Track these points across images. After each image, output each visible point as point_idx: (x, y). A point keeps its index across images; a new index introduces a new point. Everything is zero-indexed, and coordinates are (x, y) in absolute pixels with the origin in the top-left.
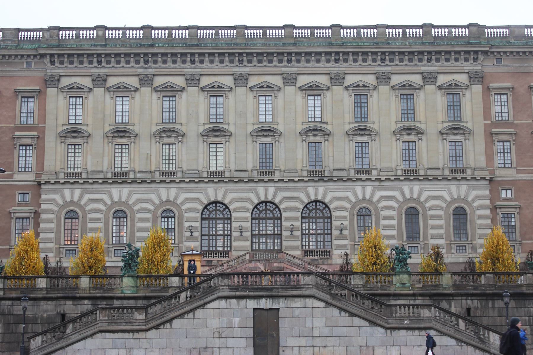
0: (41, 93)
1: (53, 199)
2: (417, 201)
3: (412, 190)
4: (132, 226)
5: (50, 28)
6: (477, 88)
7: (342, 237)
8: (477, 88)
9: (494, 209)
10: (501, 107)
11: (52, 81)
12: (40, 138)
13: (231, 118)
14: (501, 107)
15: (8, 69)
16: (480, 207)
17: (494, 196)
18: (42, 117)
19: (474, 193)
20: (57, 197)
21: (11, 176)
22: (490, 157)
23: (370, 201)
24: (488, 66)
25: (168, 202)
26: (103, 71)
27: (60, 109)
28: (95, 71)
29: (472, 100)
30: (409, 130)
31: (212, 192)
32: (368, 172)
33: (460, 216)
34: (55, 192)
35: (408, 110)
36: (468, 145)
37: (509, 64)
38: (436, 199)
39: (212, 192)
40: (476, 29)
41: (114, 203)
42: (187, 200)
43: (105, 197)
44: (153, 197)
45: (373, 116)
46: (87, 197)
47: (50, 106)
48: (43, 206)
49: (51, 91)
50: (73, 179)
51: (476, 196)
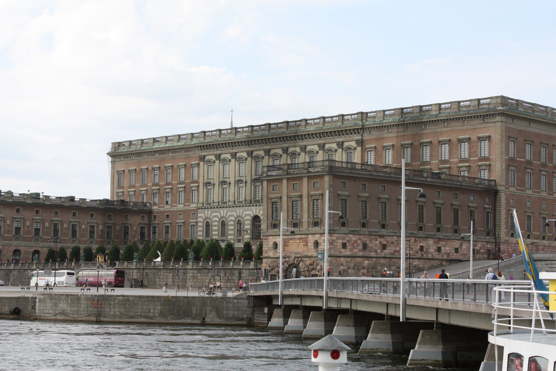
0: (198, 164)
1: (202, 215)
4: (228, 228)
6: (359, 149)
12: (198, 186)
15: (188, 153)
20: (203, 215)
21: (189, 205)
27: (201, 173)
28: (216, 152)
34: (202, 213)
37: (375, 134)
40: (363, 115)
41: (221, 217)
43: (218, 214)
44: (234, 213)
46: (213, 214)
47: (201, 171)
48: (199, 220)
49: (202, 163)
50: (208, 205)
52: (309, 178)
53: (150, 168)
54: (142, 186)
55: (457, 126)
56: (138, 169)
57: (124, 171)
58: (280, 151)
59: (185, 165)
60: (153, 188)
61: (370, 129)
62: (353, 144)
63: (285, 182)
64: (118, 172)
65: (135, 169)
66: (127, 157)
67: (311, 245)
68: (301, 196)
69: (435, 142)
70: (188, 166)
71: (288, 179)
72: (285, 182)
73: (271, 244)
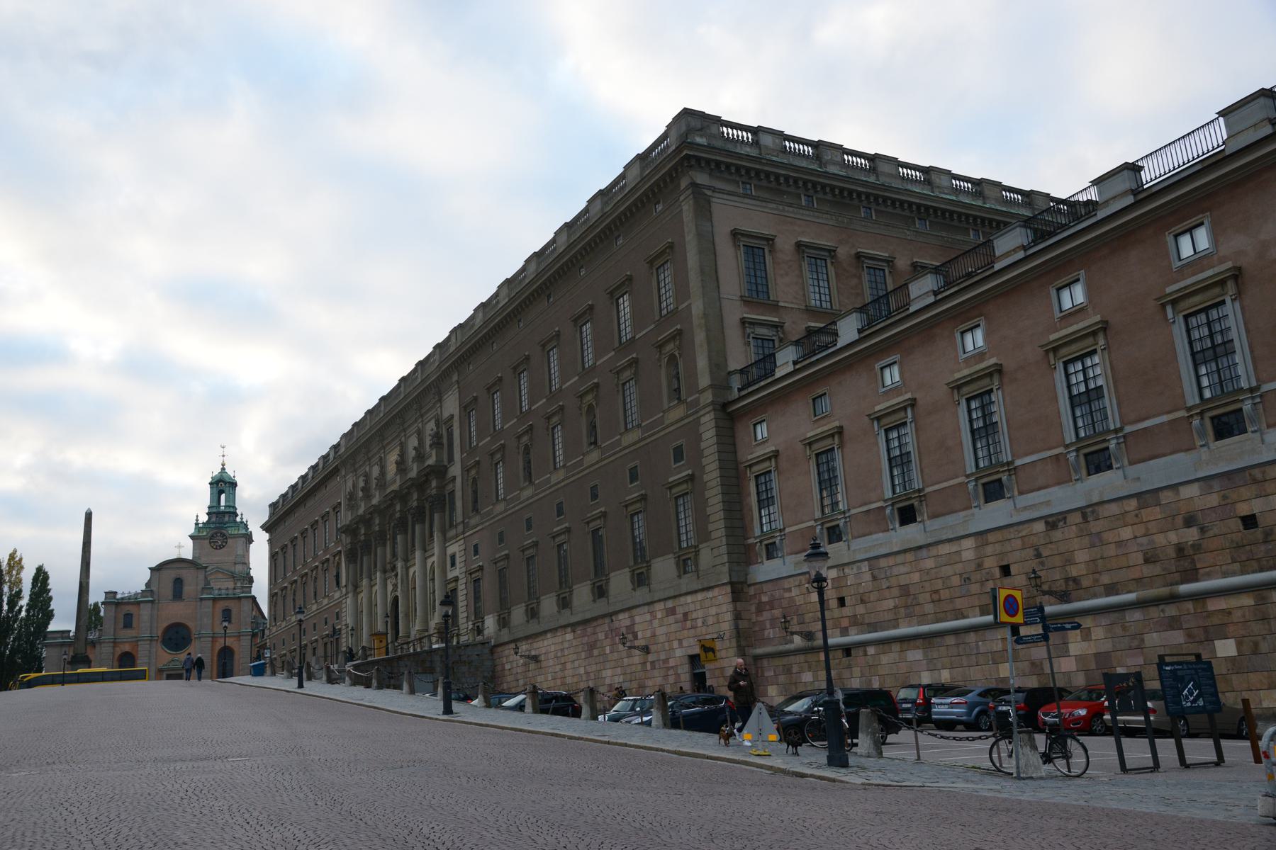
57: (770, 240)
64: (735, 234)
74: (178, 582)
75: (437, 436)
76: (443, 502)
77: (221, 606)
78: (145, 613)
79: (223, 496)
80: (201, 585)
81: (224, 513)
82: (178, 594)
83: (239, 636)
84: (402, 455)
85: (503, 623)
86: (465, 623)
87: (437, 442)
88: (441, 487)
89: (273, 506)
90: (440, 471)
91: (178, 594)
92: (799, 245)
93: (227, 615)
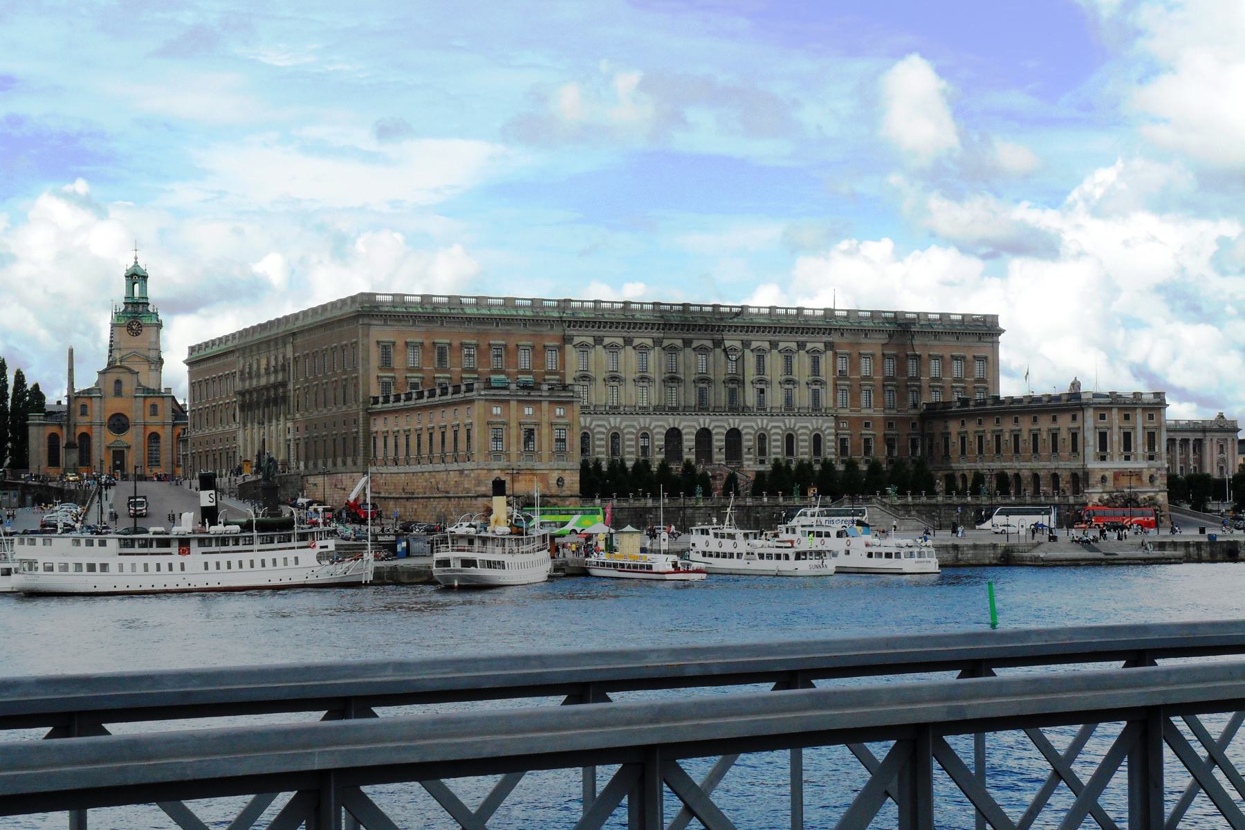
0: (561, 349)
2: (793, 429)
3: (790, 422)
5: (565, 301)
6: (830, 353)
7: (749, 453)
8: (830, 353)
9: (837, 435)
10: (841, 364)
11: (566, 340)
13: (681, 369)
14: (841, 364)
16: (829, 434)
17: (837, 427)
18: (563, 366)
19: (826, 425)
22: (835, 400)
23: (765, 429)
24: (835, 338)
25: (645, 428)
26: (601, 334)
29: (826, 361)
30: (788, 381)
31: (672, 421)
32: (765, 409)
33: (817, 440)
35: (788, 368)
36: (822, 392)
37: (848, 338)
38: (804, 427)
39: (672, 421)
42: (656, 427)
44: (635, 423)
45: (767, 371)
46: (595, 423)
47: (567, 358)
49: (568, 347)
51: (826, 426)
52: (1144, 409)
53: (456, 343)
54: (437, 371)
55: (951, 341)
56: (427, 342)
57: (394, 343)
58: (709, 344)
59: (533, 347)
60: (464, 375)
61: (841, 331)
62: (821, 346)
63: (1115, 411)
65: (422, 344)
66: (400, 321)
67: (1146, 478)
68: (1134, 428)
69: (925, 356)
70: (539, 347)
71: (1120, 409)
72: (1115, 411)
73: (1099, 477)
74: (118, 382)
75: (283, 365)
76: (285, 399)
77: (149, 401)
78: (95, 405)
79: (137, 286)
80: (135, 386)
81: (138, 304)
82: (118, 393)
83: (163, 425)
84: (268, 365)
85: (306, 466)
86: (293, 464)
87: (284, 369)
88: (284, 392)
89: (192, 349)
90: (284, 384)
91: (118, 393)
92: (406, 344)
93: (154, 410)
